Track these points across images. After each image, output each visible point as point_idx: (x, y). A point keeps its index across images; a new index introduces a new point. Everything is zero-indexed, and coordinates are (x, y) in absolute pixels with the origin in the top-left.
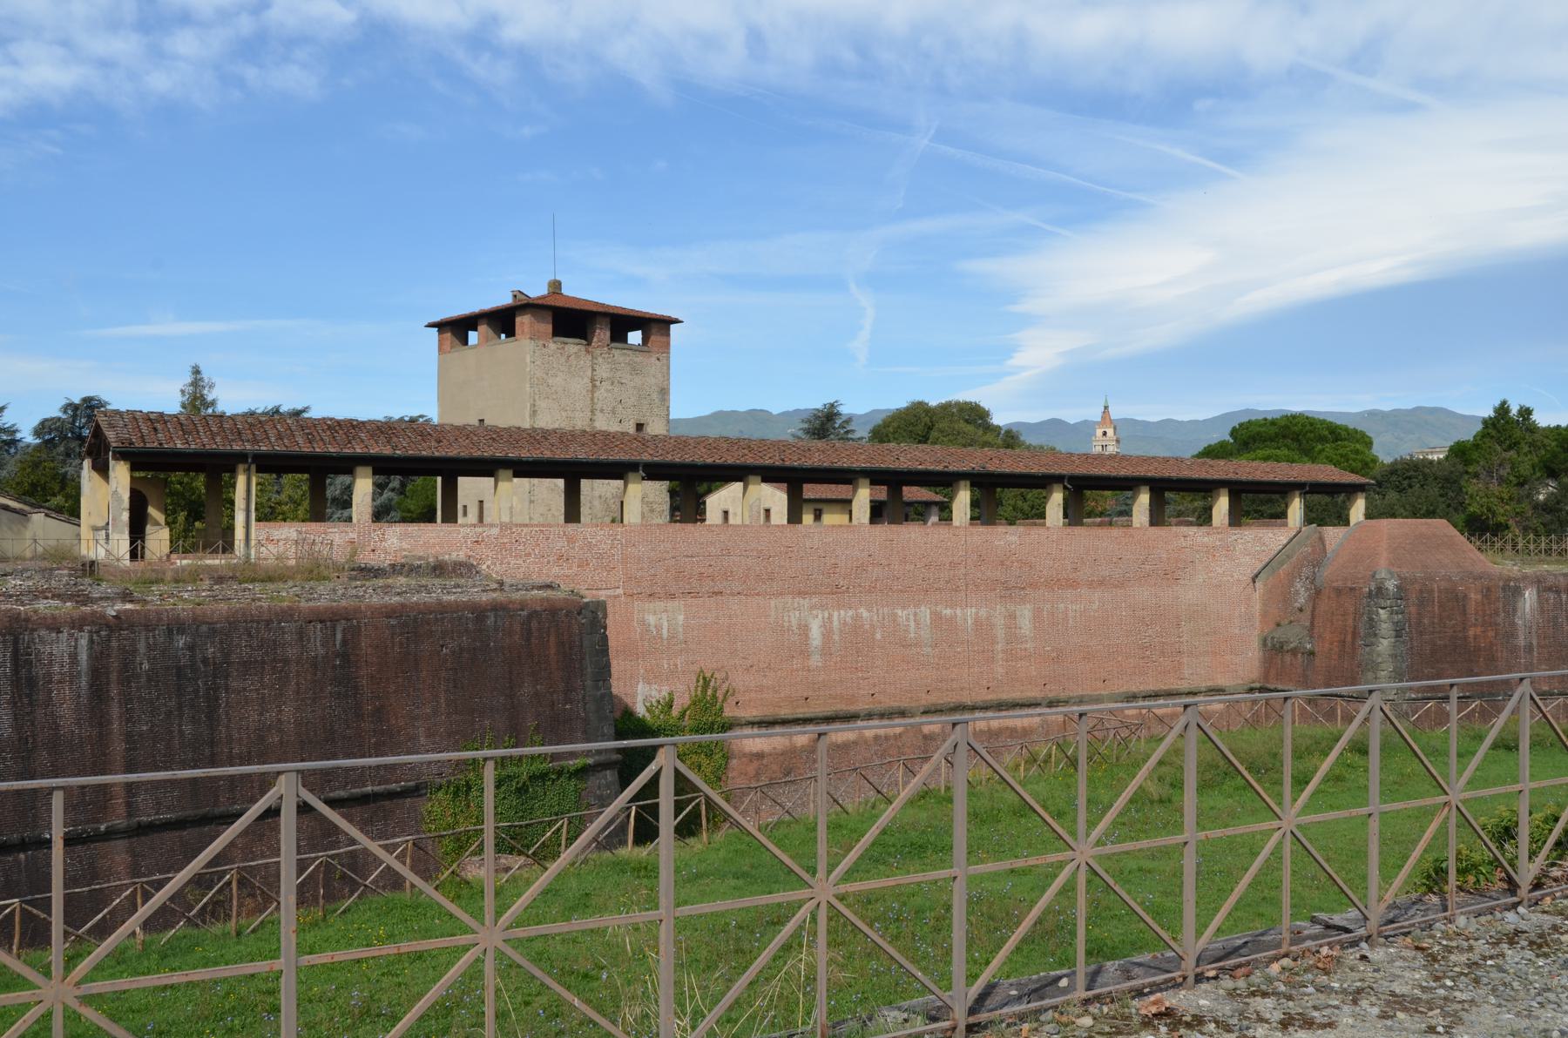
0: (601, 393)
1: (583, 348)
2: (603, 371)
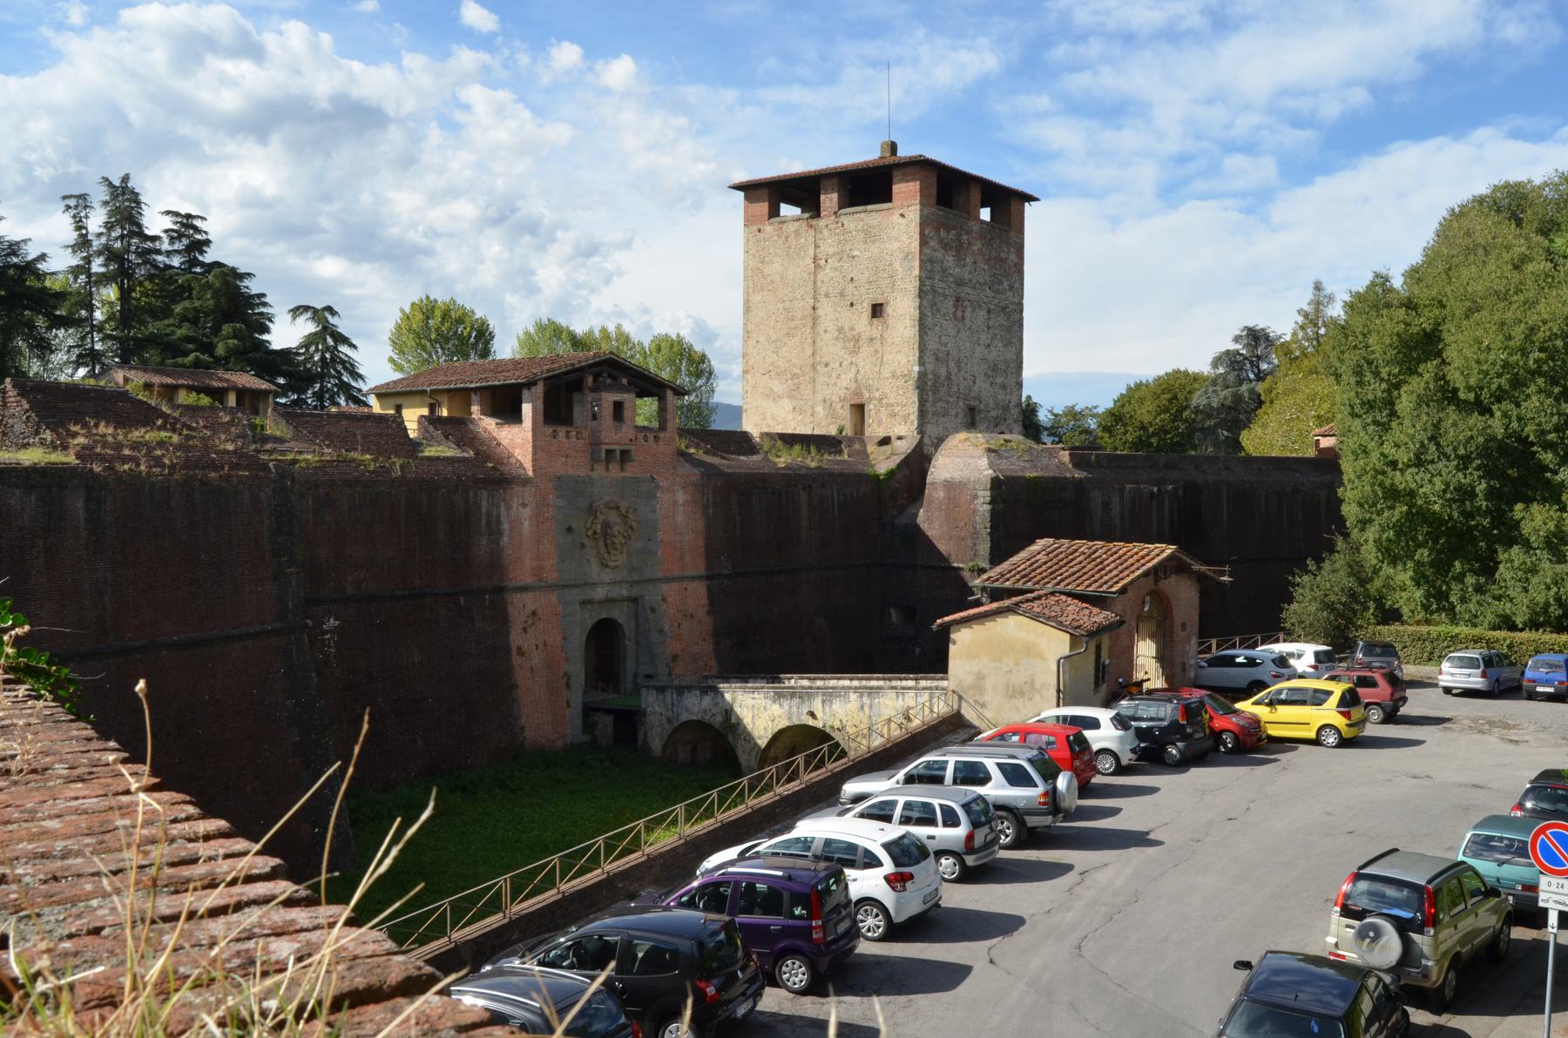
0: (826, 274)
1: (804, 224)
2: (829, 246)
